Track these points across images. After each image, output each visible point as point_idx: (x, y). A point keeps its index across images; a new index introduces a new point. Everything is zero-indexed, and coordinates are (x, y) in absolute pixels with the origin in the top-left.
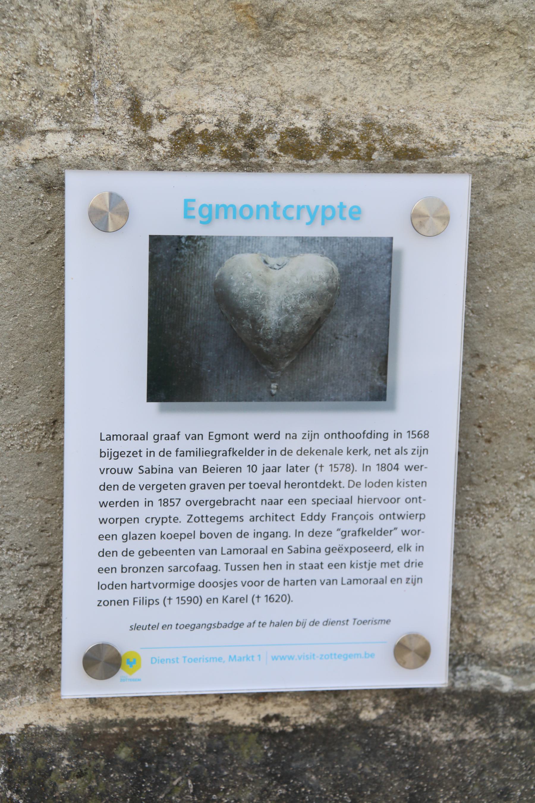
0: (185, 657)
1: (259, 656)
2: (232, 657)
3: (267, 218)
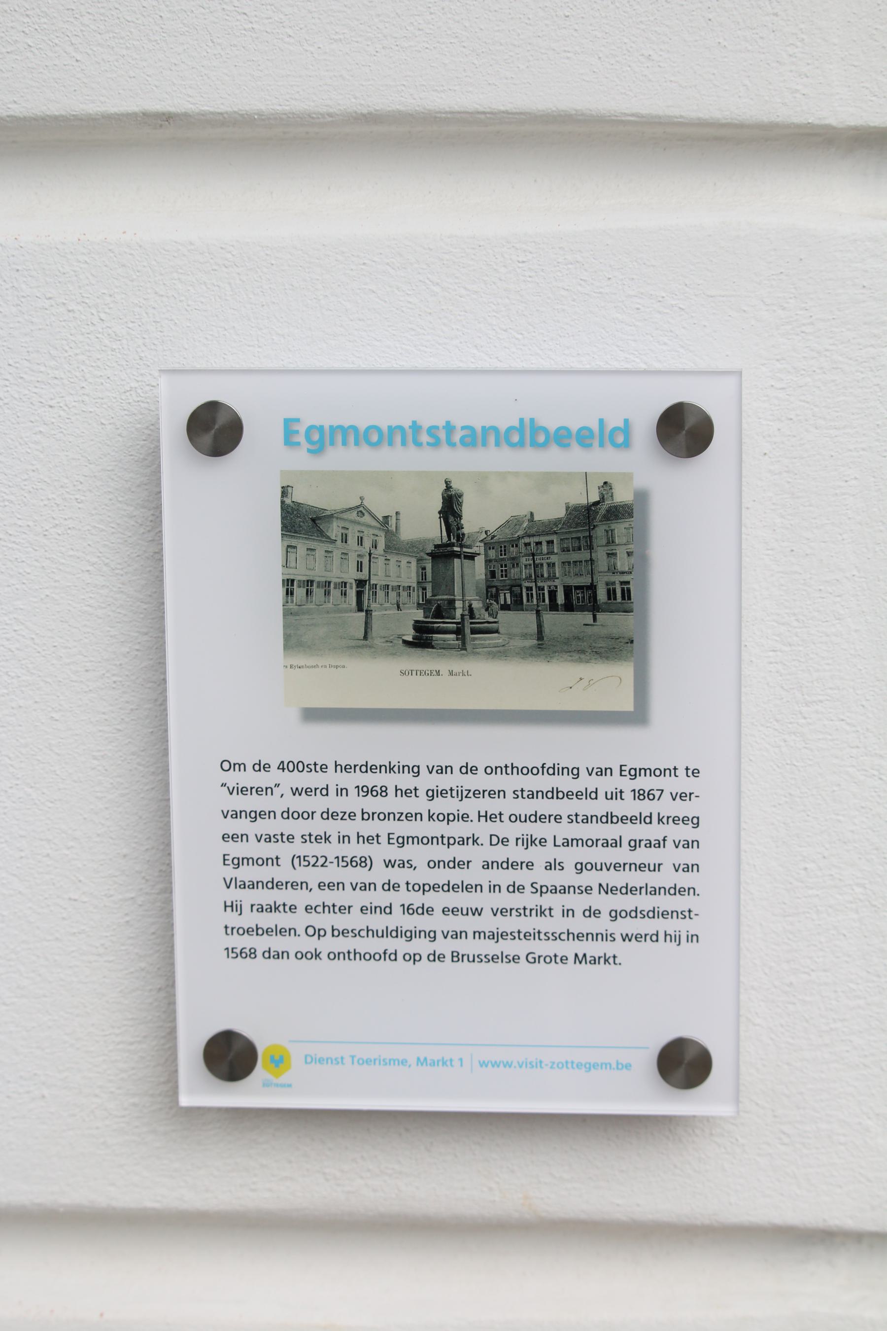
0: (353, 1057)
1: (461, 1059)
2: (422, 1059)
3: (404, 443)
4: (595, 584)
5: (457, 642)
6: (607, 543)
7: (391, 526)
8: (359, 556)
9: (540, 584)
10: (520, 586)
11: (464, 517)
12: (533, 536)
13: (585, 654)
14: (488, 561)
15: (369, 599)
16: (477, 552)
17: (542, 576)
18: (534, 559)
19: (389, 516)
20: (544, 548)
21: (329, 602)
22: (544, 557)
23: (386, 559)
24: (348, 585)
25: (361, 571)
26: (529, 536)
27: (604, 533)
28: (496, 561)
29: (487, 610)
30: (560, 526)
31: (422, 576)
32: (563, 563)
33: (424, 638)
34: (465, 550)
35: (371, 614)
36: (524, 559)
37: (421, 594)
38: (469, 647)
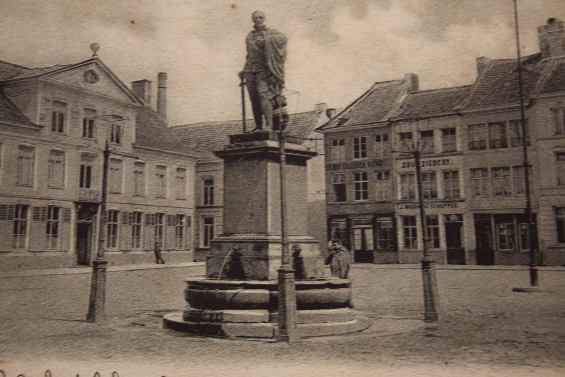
4: (534, 211)
5: (269, 325)
6: (557, 133)
7: (149, 101)
8: (85, 156)
9: (429, 211)
10: (391, 215)
11: (287, 85)
12: (418, 119)
13: (516, 347)
14: (331, 167)
15: (101, 241)
16: (312, 150)
17: (434, 195)
18: (418, 163)
19: (144, 81)
20: (438, 138)
21: (22, 247)
22: (437, 159)
23: (136, 163)
24: (60, 213)
25: (88, 186)
26: (408, 120)
27: (549, 115)
28: (347, 166)
29: (328, 261)
30: (467, 101)
31: (206, 194)
32: (473, 170)
33: (207, 317)
34: (288, 146)
35: (104, 270)
36: (400, 163)
37: (202, 227)
38: (293, 333)
